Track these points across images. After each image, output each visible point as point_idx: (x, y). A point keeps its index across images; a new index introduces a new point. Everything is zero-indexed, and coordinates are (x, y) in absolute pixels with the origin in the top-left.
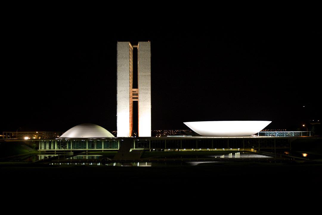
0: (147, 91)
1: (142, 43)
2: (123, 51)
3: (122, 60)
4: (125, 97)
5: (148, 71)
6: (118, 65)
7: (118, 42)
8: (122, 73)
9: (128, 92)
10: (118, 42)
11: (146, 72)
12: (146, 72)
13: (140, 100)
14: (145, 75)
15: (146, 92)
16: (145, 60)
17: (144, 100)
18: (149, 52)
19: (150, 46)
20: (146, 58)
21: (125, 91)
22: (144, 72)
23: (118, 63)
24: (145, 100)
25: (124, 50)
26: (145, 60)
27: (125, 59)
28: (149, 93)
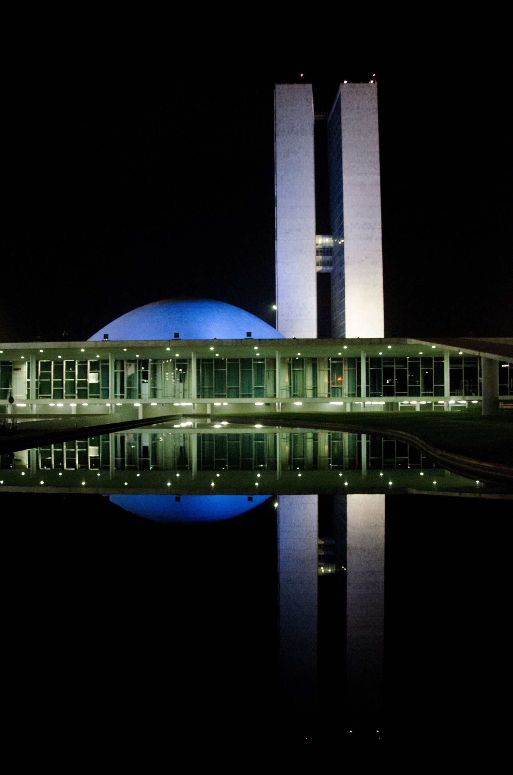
1: (351, 87)
2: (293, 110)
3: (290, 137)
4: (301, 250)
6: (277, 154)
7: (277, 86)
10: (277, 86)
11: (366, 174)
12: (366, 174)
13: (348, 257)
17: (363, 261)
18: (373, 113)
19: (376, 97)
21: (299, 230)
22: (358, 174)
23: (278, 146)
24: (363, 258)
25: (294, 111)
28: (377, 239)
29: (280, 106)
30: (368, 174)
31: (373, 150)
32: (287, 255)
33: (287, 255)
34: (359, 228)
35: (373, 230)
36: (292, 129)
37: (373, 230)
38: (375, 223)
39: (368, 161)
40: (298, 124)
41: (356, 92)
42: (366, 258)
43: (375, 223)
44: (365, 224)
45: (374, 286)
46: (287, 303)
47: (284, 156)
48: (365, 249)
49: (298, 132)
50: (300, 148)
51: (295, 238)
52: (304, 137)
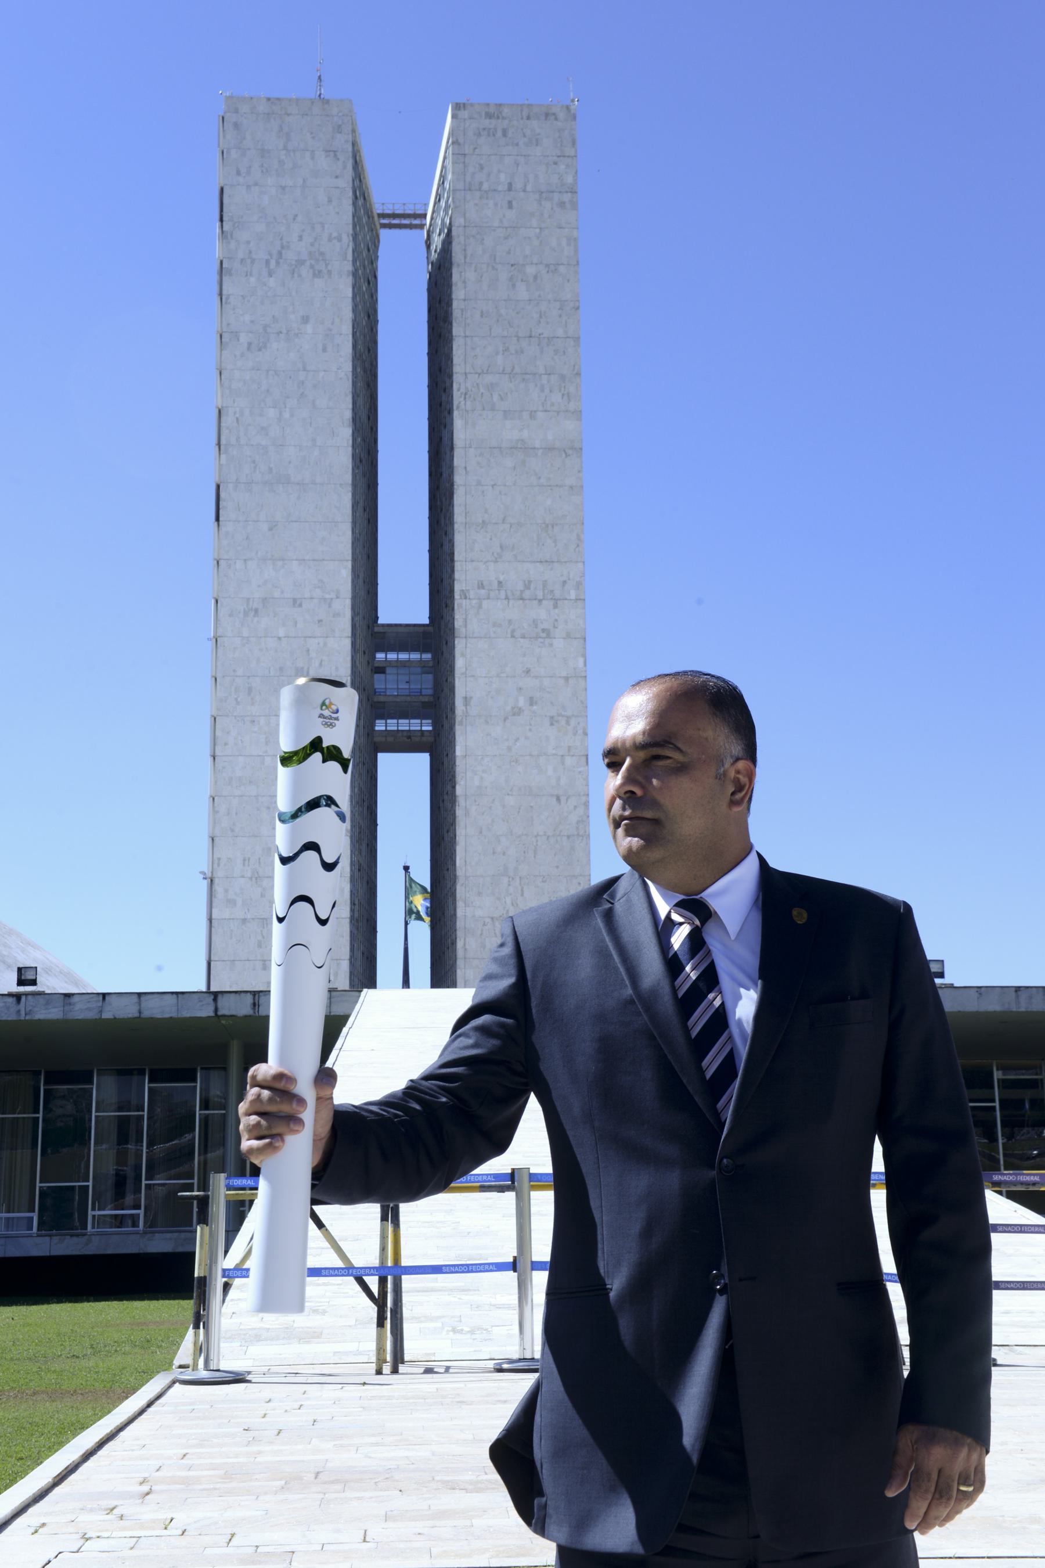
0: (542, 614)
2: (283, 188)
3: (272, 282)
5: (556, 398)
8: (272, 413)
9: (337, 615)
12: (532, 415)
13: (467, 700)
14: (523, 448)
15: (535, 623)
16: (522, 292)
17: (517, 712)
18: (562, 204)
20: (530, 270)
21: (296, 603)
24: (522, 702)
26: (522, 292)
27: (305, 271)
28: (568, 636)
29: (238, 173)
30: (540, 414)
31: (560, 332)
32: (250, 690)
33: (250, 690)
34: (507, 598)
35: (555, 606)
36: (280, 254)
37: (555, 606)
38: (564, 582)
39: (542, 370)
40: (301, 238)
41: (505, 133)
42: (532, 702)
43: (564, 582)
44: (527, 587)
45: (558, 799)
46: (245, 861)
47: (250, 344)
48: (528, 671)
49: (301, 263)
50: (305, 320)
51: (281, 634)
52: (319, 282)
